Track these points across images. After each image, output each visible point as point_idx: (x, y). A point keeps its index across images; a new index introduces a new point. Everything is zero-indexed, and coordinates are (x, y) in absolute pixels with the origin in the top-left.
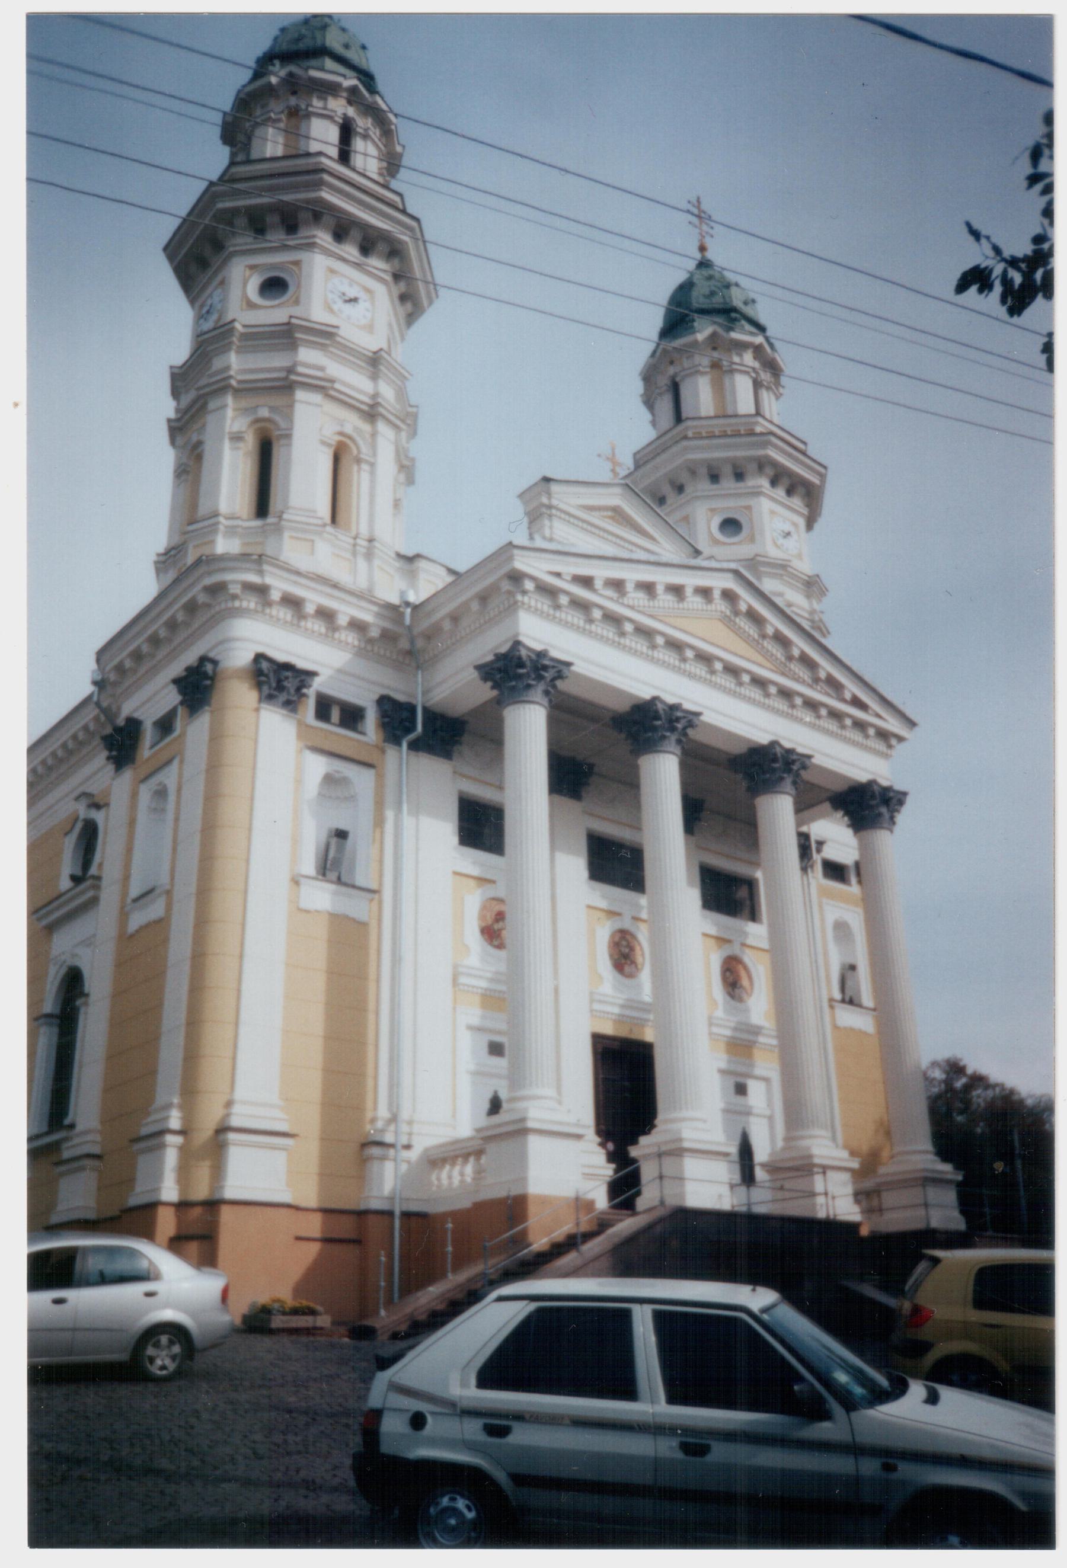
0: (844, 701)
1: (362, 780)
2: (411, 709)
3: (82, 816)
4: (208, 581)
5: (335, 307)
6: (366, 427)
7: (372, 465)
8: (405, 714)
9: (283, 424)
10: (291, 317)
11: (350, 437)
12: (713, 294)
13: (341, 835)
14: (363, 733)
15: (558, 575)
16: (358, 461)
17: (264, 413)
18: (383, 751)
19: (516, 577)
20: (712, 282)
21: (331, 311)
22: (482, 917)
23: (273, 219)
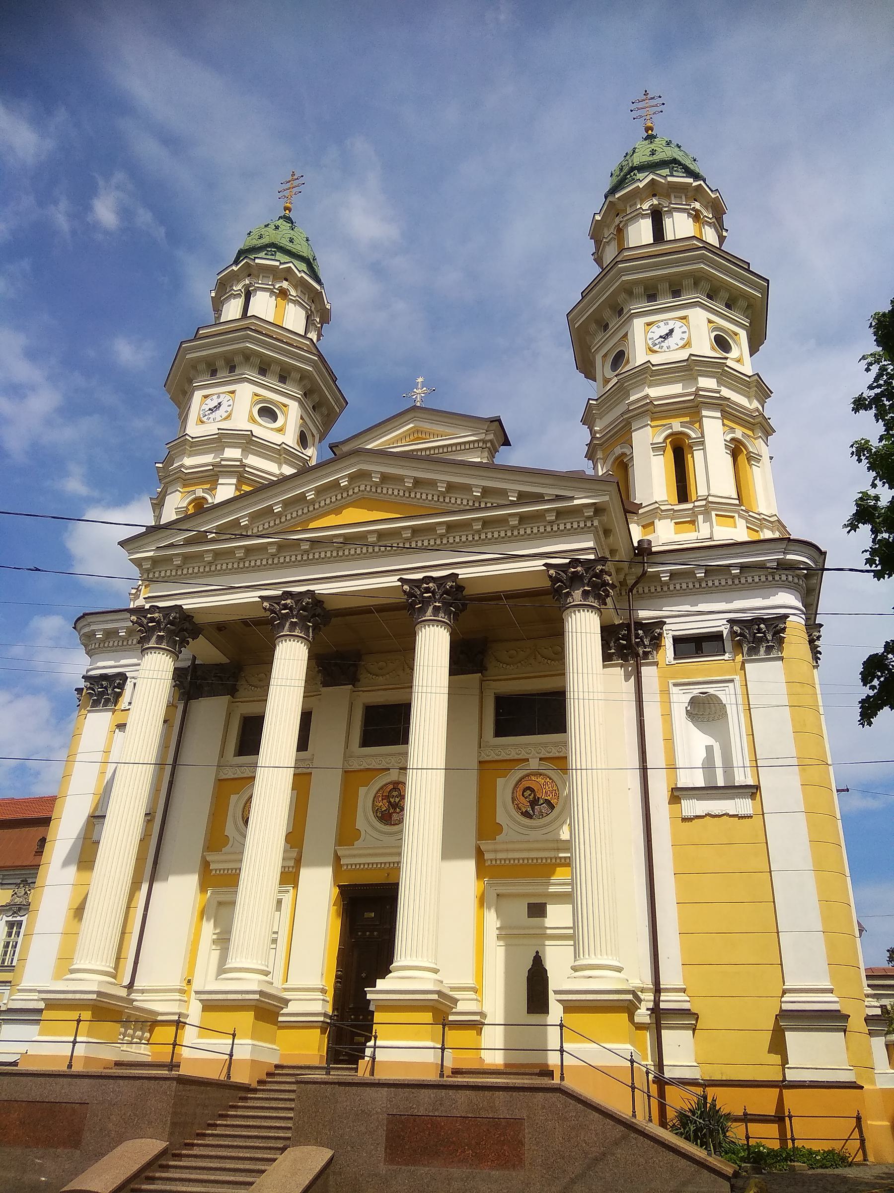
6: (750, 433)
9: (694, 435)
10: (691, 355)
16: (749, 459)
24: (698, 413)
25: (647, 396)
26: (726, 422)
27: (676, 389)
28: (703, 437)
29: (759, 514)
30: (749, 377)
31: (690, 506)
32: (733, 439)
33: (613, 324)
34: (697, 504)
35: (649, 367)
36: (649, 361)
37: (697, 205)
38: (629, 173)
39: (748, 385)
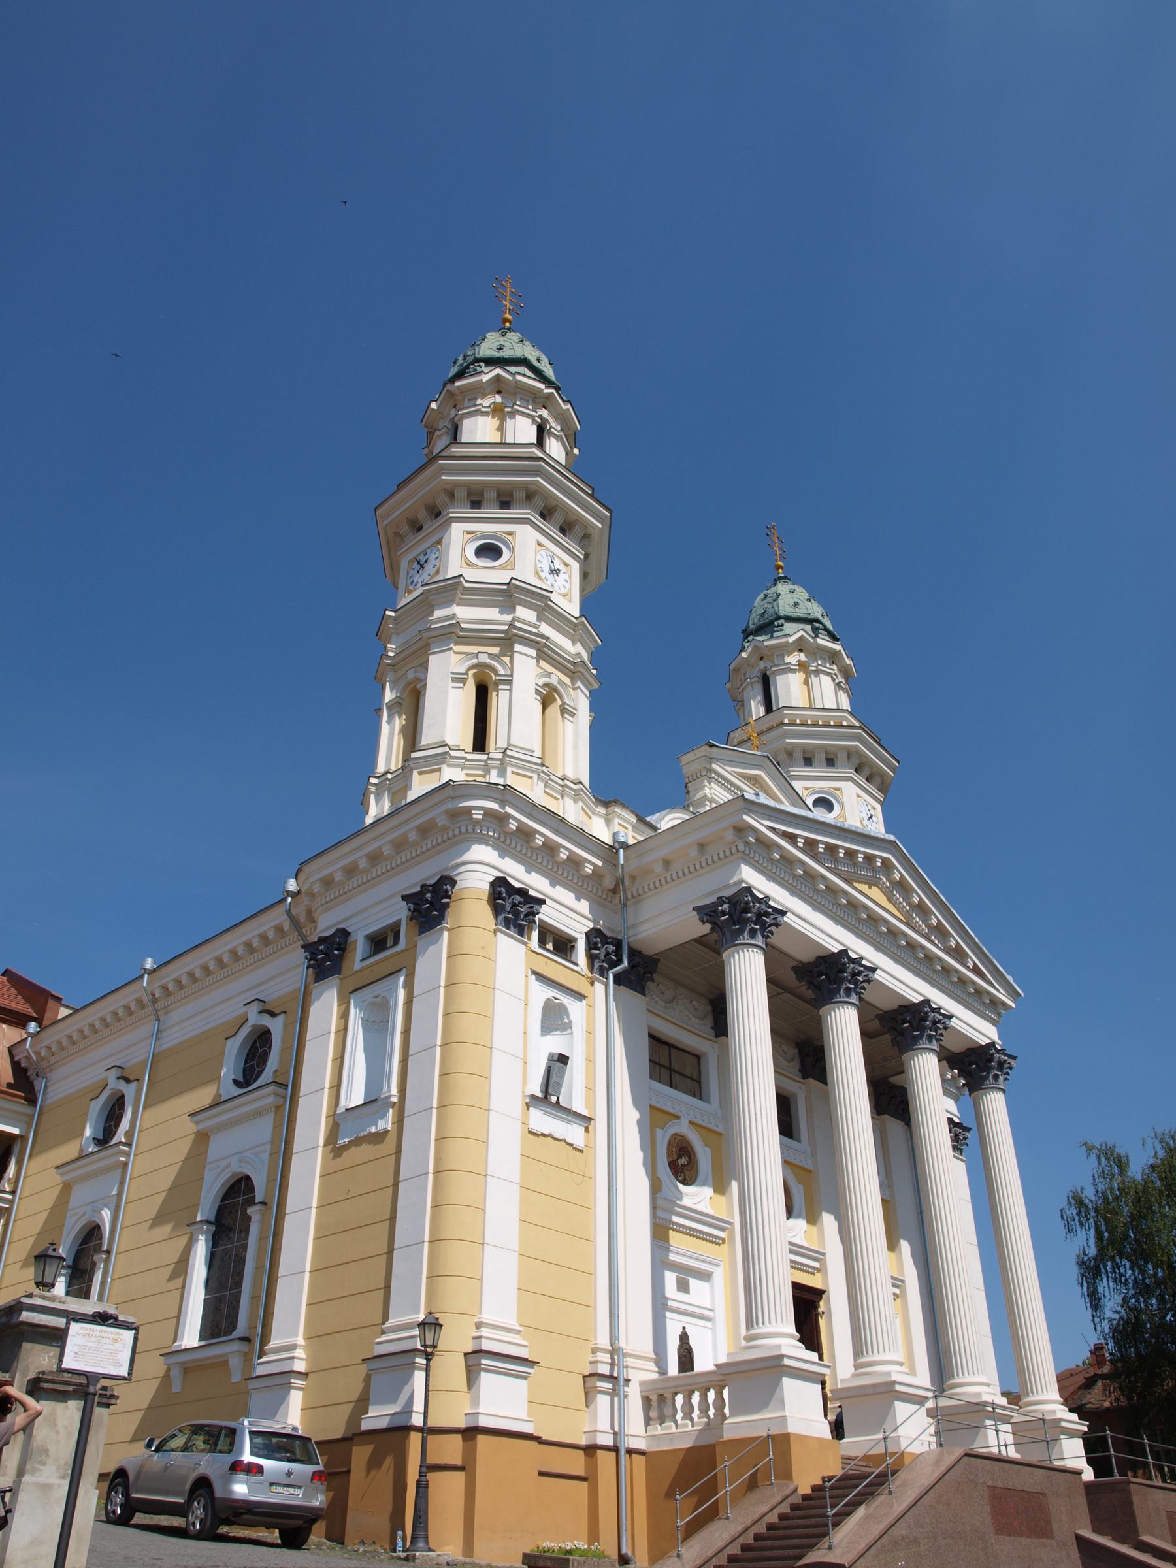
0: (967, 968)
1: (576, 1009)
2: (618, 944)
3: (251, 1022)
4: (450, 805)
5: (543, 575)
6: (567, 681)
7: (573, 715)
8: (612, 948)
9: (502, 672)
10: (512, 578)
11: (555, 690)
12: (796, 604)
13: (563, 1059)
14: (576, 964)
15: (773, 830)
16: (563, 711)
17: (484, 659)
18: (592, 984)
19: (742, 830)
20: (794, 595)
21: (540, 578)
22: (669, 1152)
23: (491, 495)
24: (512, 646)
25: (453, 616)
26: (542, 663)
27: (492, 614)
28: (511, 675)
29: (562, 780)
30: (576, 618)
31: (483, 757)
32: (546, 685)
33: (429, 526)
34: (491, 756)
35: (460, 582)
36: (461, 575)
37: (545, 413)
38: (472, 363)
39: (574, 627)
